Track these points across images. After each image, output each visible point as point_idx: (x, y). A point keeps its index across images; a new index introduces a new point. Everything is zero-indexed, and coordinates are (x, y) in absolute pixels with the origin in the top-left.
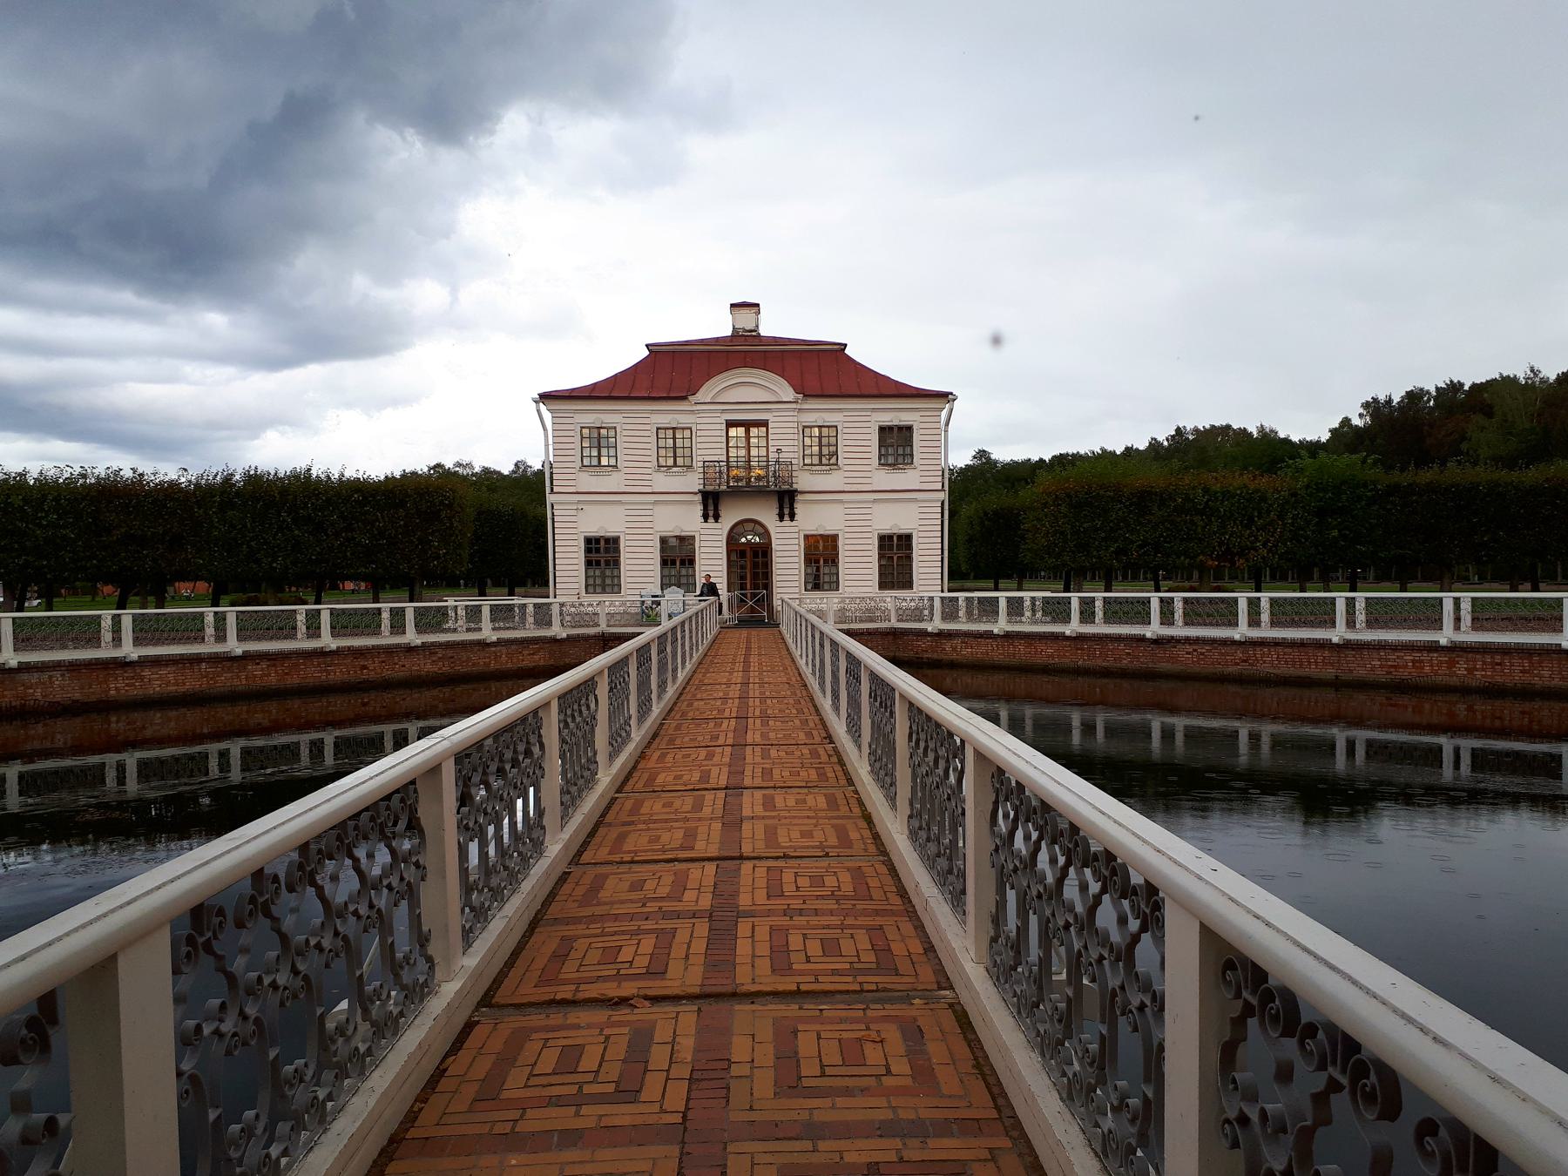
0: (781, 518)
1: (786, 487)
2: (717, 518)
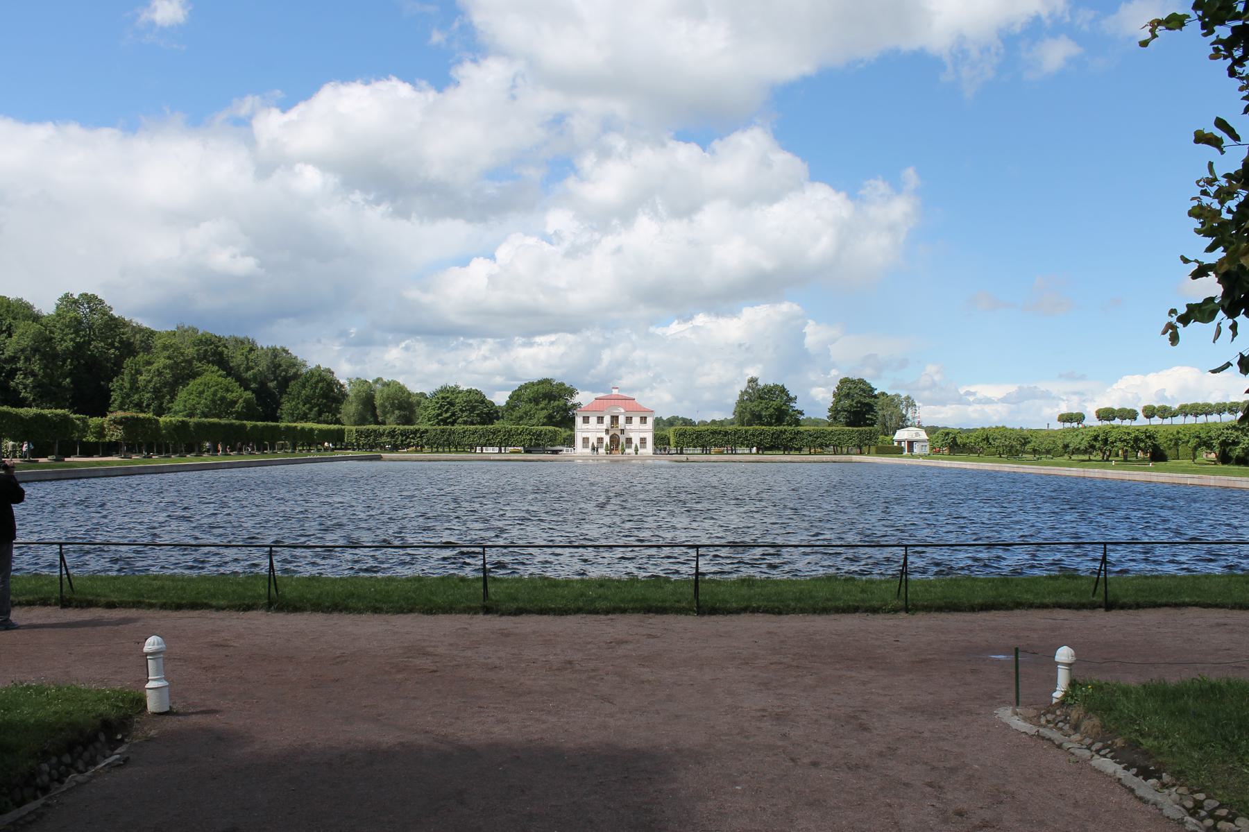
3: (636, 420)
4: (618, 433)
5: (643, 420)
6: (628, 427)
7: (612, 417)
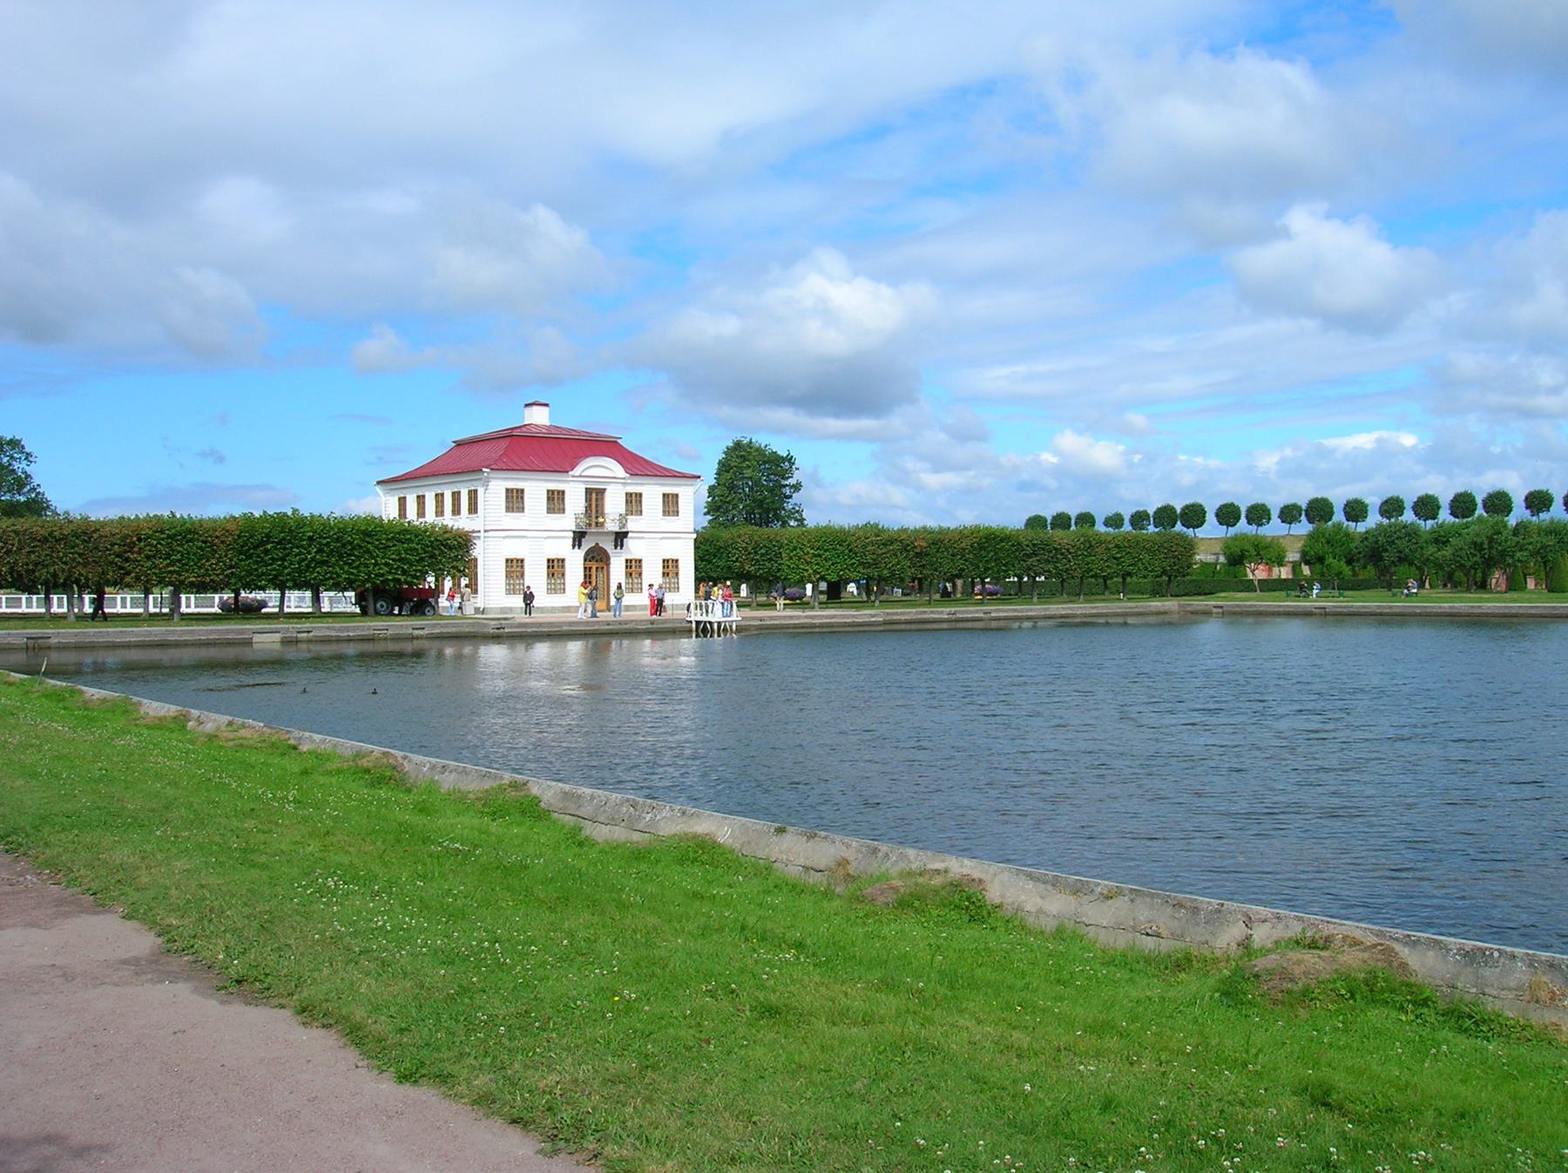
0: (616, 548)
4: (608, 546)
5: (670, 504)
7: (589, 492)
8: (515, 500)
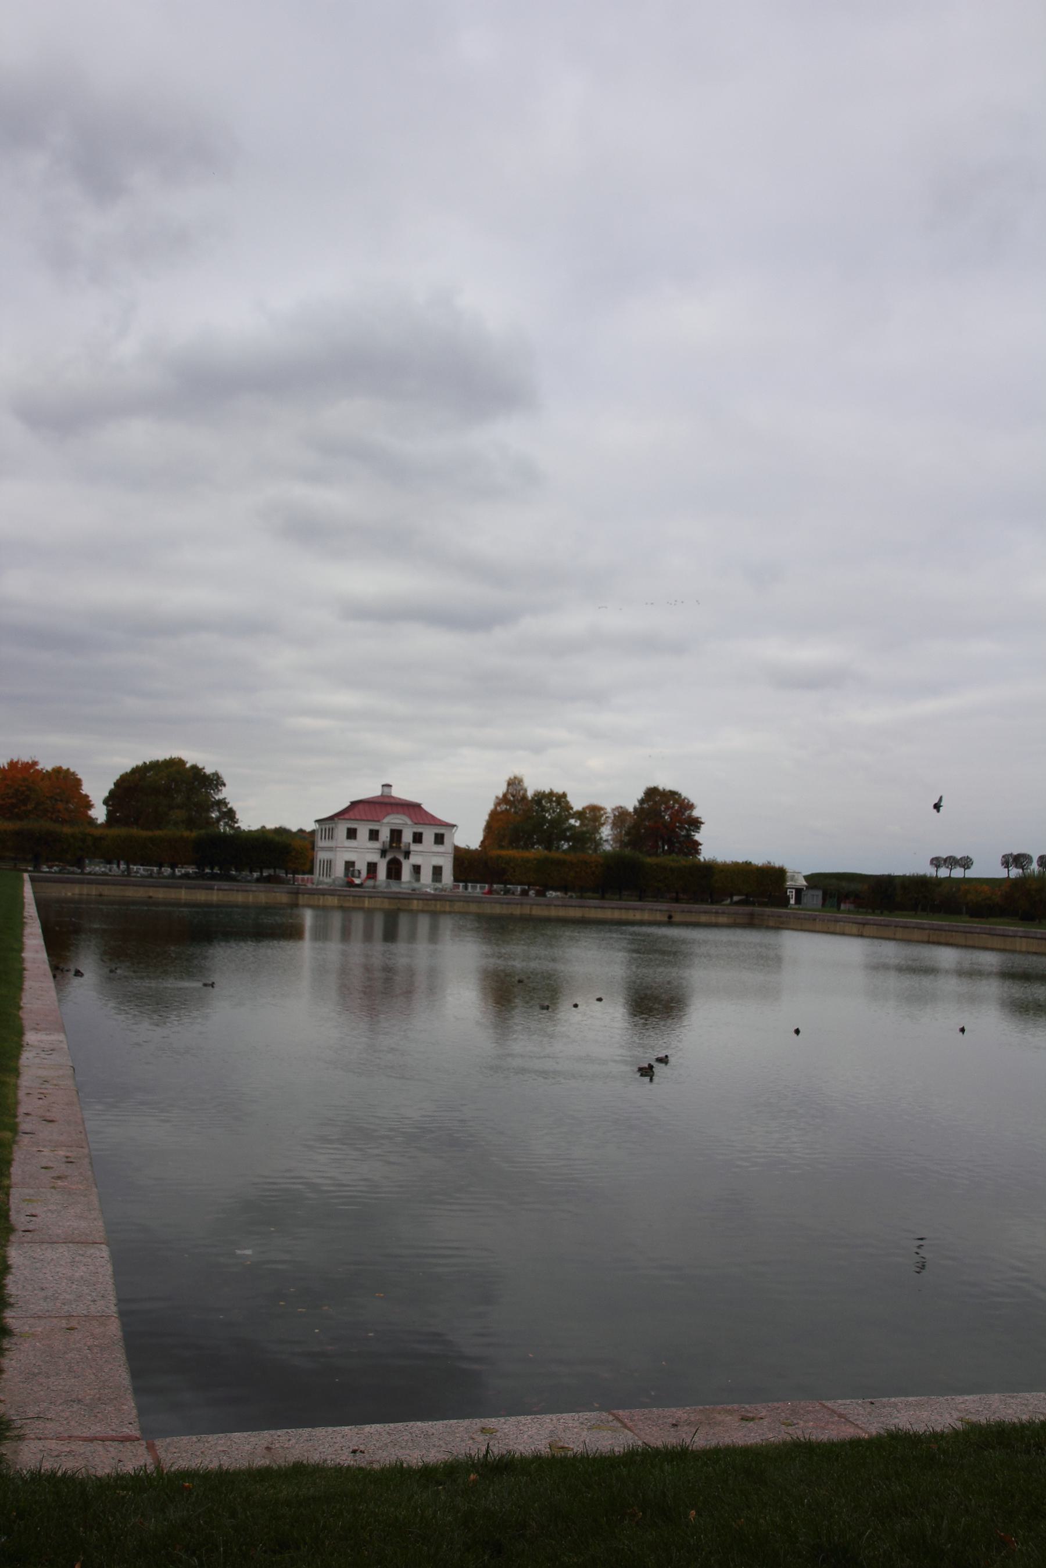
0: (405, 858)
1: (407, 850)
2: (385, 857)
3: (429, 836)
4: (401, 858)
6: (414, 847)
7: (393, 832)
8: (352, 834)
